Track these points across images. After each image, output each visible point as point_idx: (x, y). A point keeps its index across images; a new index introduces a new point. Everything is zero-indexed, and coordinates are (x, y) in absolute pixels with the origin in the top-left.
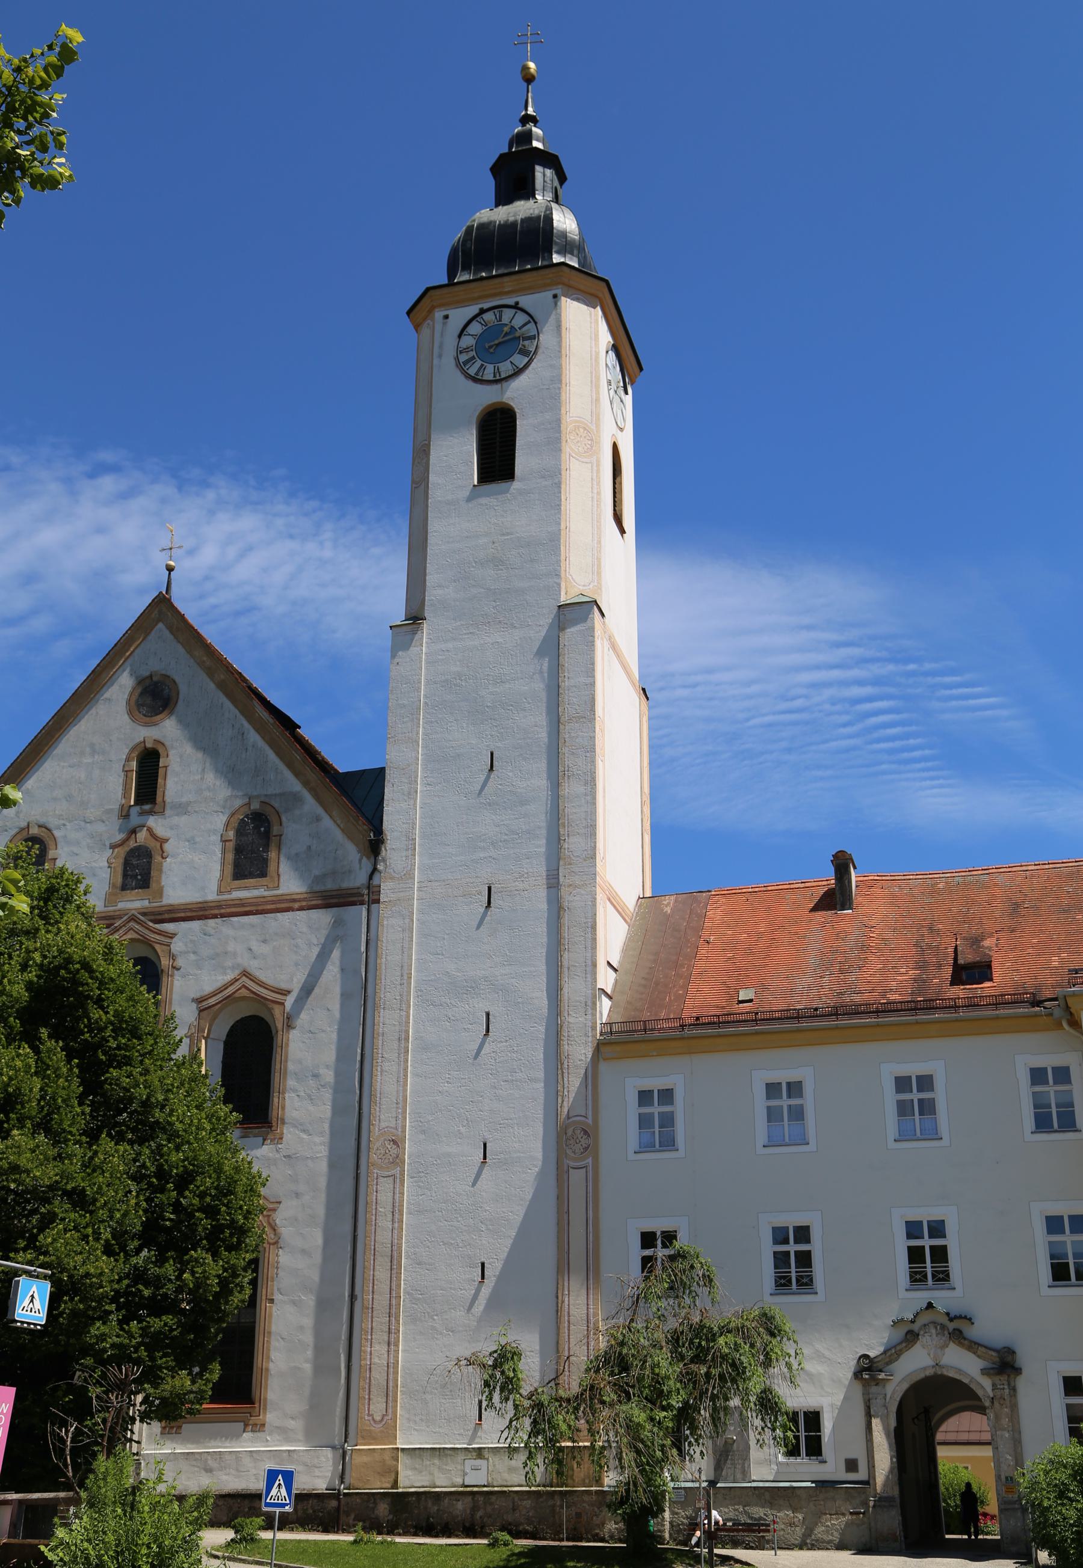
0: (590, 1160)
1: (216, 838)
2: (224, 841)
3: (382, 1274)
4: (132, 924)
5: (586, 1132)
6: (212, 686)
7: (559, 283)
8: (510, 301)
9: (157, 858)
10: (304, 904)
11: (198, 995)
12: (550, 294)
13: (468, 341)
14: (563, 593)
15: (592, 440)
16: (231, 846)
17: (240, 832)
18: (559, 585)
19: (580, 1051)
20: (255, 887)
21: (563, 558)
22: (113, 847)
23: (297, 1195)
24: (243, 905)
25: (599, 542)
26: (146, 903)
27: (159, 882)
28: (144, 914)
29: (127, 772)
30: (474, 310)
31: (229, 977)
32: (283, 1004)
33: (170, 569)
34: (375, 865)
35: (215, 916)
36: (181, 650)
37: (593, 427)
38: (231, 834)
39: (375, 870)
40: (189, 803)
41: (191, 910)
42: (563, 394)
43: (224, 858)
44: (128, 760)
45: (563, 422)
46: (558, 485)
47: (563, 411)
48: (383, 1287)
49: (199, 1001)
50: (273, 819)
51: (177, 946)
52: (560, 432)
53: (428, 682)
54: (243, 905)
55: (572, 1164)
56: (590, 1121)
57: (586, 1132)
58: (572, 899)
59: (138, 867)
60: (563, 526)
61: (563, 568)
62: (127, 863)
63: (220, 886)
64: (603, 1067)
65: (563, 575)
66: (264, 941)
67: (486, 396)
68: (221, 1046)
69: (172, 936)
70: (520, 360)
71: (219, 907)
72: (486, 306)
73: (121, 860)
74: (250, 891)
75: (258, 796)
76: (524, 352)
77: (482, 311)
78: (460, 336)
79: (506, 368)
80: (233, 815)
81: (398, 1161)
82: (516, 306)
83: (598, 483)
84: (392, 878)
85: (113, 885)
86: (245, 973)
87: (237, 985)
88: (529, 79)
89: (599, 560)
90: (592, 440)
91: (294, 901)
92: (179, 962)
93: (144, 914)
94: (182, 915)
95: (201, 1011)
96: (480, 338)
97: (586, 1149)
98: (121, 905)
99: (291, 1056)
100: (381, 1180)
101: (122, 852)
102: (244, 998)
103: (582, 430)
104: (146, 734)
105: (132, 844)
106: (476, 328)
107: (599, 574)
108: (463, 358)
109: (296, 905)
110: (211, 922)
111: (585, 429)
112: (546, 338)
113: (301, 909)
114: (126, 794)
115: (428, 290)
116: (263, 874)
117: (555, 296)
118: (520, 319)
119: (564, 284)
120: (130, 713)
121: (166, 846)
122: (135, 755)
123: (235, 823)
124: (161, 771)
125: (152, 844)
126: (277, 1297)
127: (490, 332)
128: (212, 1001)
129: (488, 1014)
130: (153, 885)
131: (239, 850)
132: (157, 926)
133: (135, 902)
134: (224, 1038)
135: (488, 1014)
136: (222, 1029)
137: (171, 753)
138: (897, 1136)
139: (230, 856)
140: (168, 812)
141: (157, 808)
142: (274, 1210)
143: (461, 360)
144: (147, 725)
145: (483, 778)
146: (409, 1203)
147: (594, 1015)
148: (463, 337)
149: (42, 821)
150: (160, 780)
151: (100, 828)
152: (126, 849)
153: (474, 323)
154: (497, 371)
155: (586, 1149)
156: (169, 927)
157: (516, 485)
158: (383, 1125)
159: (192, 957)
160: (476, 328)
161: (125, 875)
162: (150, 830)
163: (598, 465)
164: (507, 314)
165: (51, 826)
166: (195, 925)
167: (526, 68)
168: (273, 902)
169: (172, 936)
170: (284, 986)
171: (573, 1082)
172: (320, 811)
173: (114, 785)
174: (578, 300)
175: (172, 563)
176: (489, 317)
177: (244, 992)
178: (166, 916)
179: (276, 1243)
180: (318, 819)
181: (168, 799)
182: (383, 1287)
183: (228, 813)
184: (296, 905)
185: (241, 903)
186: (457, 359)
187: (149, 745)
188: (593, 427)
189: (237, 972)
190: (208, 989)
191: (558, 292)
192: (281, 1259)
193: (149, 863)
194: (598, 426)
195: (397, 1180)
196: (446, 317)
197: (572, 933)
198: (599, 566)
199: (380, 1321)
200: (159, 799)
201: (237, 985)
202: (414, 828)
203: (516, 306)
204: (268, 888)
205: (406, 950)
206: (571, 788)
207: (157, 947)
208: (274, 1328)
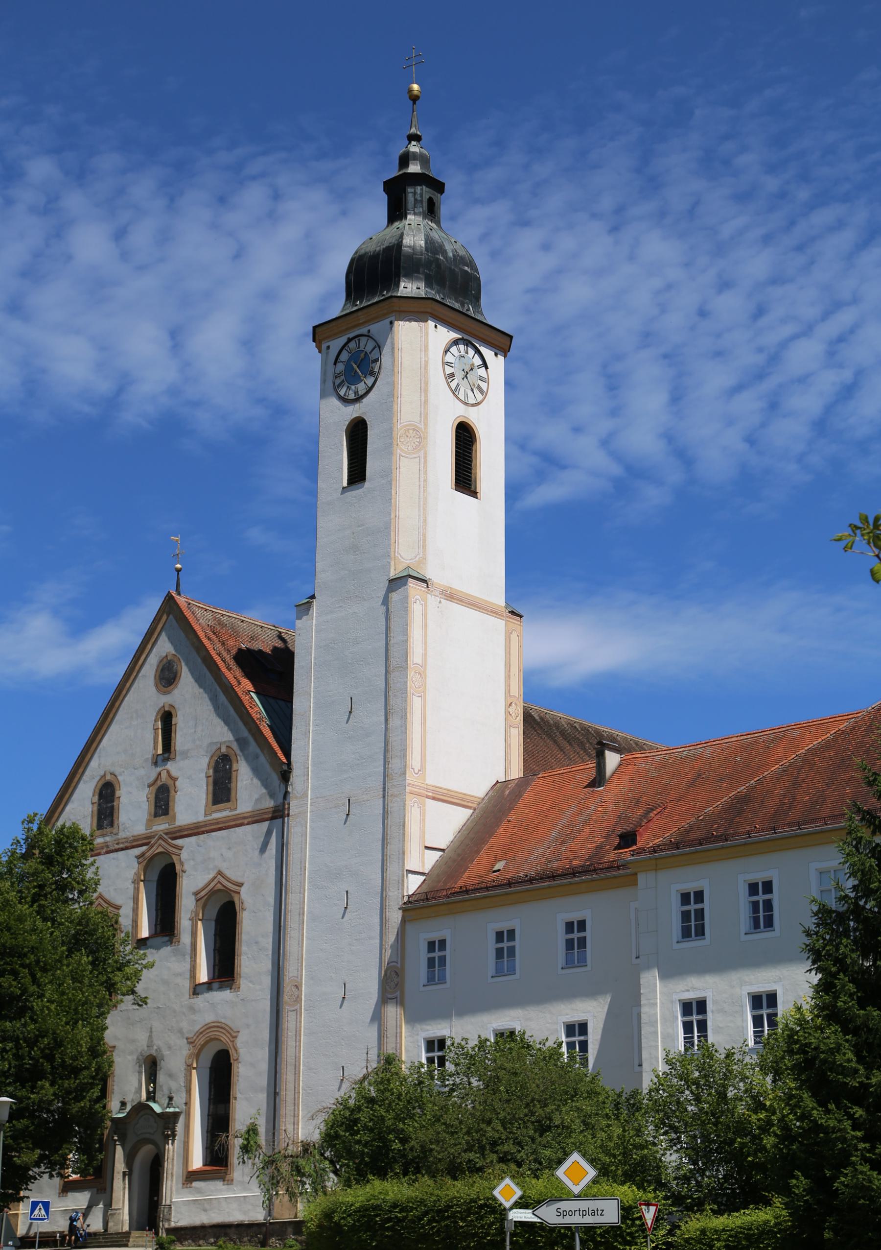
0: (398, 993)
1: (203, 775)
2: (208, 777)
3: (290, 1077)
4: (161, 841)
5: (397, 973)
6: (200, 660)
7: (392, 312)
8: (364, 331)
9: (172, 793)
10: (250, 820)
11: (195, 890)
12: (387, 321)
13: (341, 367)
14: (392, 570)
15: (420, 437)
16: (211, 779)
17: (216, 770)
18: (390, 563)
19: (395, 917)
20: (224, 810)
21: (393, 541)
22: (149, 786)
23: (248, 1026)
24: (218, 823)
25: (425, 521)
26: (167, 826)
27: (173, 810)
28: (166, 834)
29: (156, 730)
30: (343, 340)
31: (211, 876)
32: (239, 893)
33: (178, 570)
34: (286, 788)
35: (203, 833)
36: (183, 635)
37: (422, 426)
38: (211, 772)
39: (286, 794)
40: (188, 751)
41: (191, 829)
42: (395, 406)
43: (207, 789)
44: (156, 721)
45: (395, 429)
46: (390, 483)
47: (395, 420)
48: (290, 1086)
49: (196, 894)
50: (233, 758)
51: (184, 855)
52: (391, 438)
53: (317, 647)
54: (218, 823)
55: (390, 996)
56: (399, 965)
57: (397, 973)
58: (393, 807)
59: (162, 800)
60: (393, 516)
61: (392, 550)
62: (157, 797)
63: (205, 811)
64: (409, 927)
65: (392, 555)
66: (229, 849)
67: (351, 412)
68: (213, 923)
69: (180, 848)
70: (370, 381)
71: (206, 826)
72: (351, 335)
73: (154, 795)
74: (222, 813)
75: (225, 742)
76: (372, 373)
77: (349, 340)
78: (335, 364)
79: (361, 388)
80: (212, 757)
81: (298, 999)
82: (368, 336)
83: (425, 472)
84: (296, 797)
85: (149, 814)
86: (220, 873)
87: (216, 881)
88: (414, 99)
89: (424, 535)
90: (420, 437)
91: (245, 818)
92: (186, 867)
93: (166, 834)
94: (186, 833)
95: (197, 901)
96: (348, 365)
97: (397, 985)
98: (155, 828)
99: (243, 931)
100: (290, 1013)
101: (154, 789)
102: (219, 890)
103: (411, 431)
104: (164, 700)
105: (159, 783)
106: (345, 356)
107: (424, 546)
108: (338, 381)
109: (246, 821)
110: (201, 836)
111: (414, 430)
112: (385, 359)
113: (248, 824)
114: (155, 748)
115: (315, 328)
116: (228, 800)
117: (391, 323)
118: (371, 345)
119: (396, 311)
120: (156, 686)
121: (177, 783)
122: (159, 717)
123: (213, 764)
124: (173, 727)
125: (170, 782)
126: (238, 1095)
127: (354, 356)
128: (203, 894)
129: (347, 892)
130: (171, 812)
131: (216, 783)
132: (174, 842)
133: (161, 826)
134: (215, 918)
135: (347, 892)
136: (213, 912)
137: (179, 713)
138: (564, 964)
139: (211, 788)
140: (178, 758)
141: (172, 756)
142: (236, 1037)
143: (336, 384)
144: (165, 693)
145: (346, 717)
146: (305, 1028)
147: (403, 889)
148: (338, 364)
149: (112, 770)
150: (173, 735)
151: (142, 772)
152: (156, 787)
153: (344, 352)
154: (356, 393)
155: (397, 985)
156: (179, 842)
157: (367, 484)
158: (291, 975)
159: (192, 863)
160: (345, 356)
161: (156, 807)
162: (168, 772)
163: (425, 457)
164: (363, 340)
165: (117, 773)
166: (193, 839)
167: (410, 91)
168: (234, 820)
169: (180, 848)
170: (240, 880)
171: (391, 938)
172: (258, 751)
173: (148, 739)
174: (410, 320)
175: (179, 566)
176: (352, 345)
177: (219, 886)
178: (178, 834)
179: (237, 1059)
180: (257, 757)
181: (177, 749)
182: (290, 1086)
183: (209, 755)
184: (246, 821)
185: (217, 822)
186: (334, 383)
187: (166, 709)
188: (422, 426)
189: (216, 872)
190: (201, 885)
191: (392, 318)
192: (240, 1070)
193: (168, 796)
194: (426, 424)
195: (298, 1012)
196: (328, 347)
197: (393, 831)
198: (425, 541)
199: (290, 1107)
200: (172, 749)
201: (216, 881)
202: (308, 760)
203: (368, 336)
204: (231, 810)
205: (303, 850)
206: (394, 722)
207: (174, 856)
208: (237, 1117)
